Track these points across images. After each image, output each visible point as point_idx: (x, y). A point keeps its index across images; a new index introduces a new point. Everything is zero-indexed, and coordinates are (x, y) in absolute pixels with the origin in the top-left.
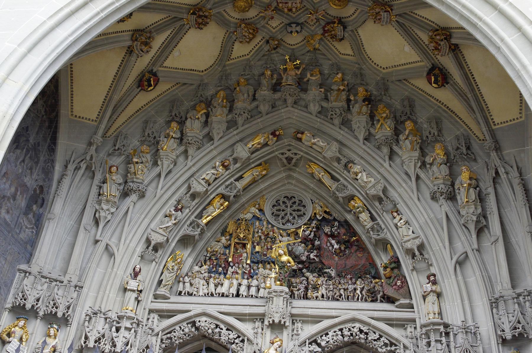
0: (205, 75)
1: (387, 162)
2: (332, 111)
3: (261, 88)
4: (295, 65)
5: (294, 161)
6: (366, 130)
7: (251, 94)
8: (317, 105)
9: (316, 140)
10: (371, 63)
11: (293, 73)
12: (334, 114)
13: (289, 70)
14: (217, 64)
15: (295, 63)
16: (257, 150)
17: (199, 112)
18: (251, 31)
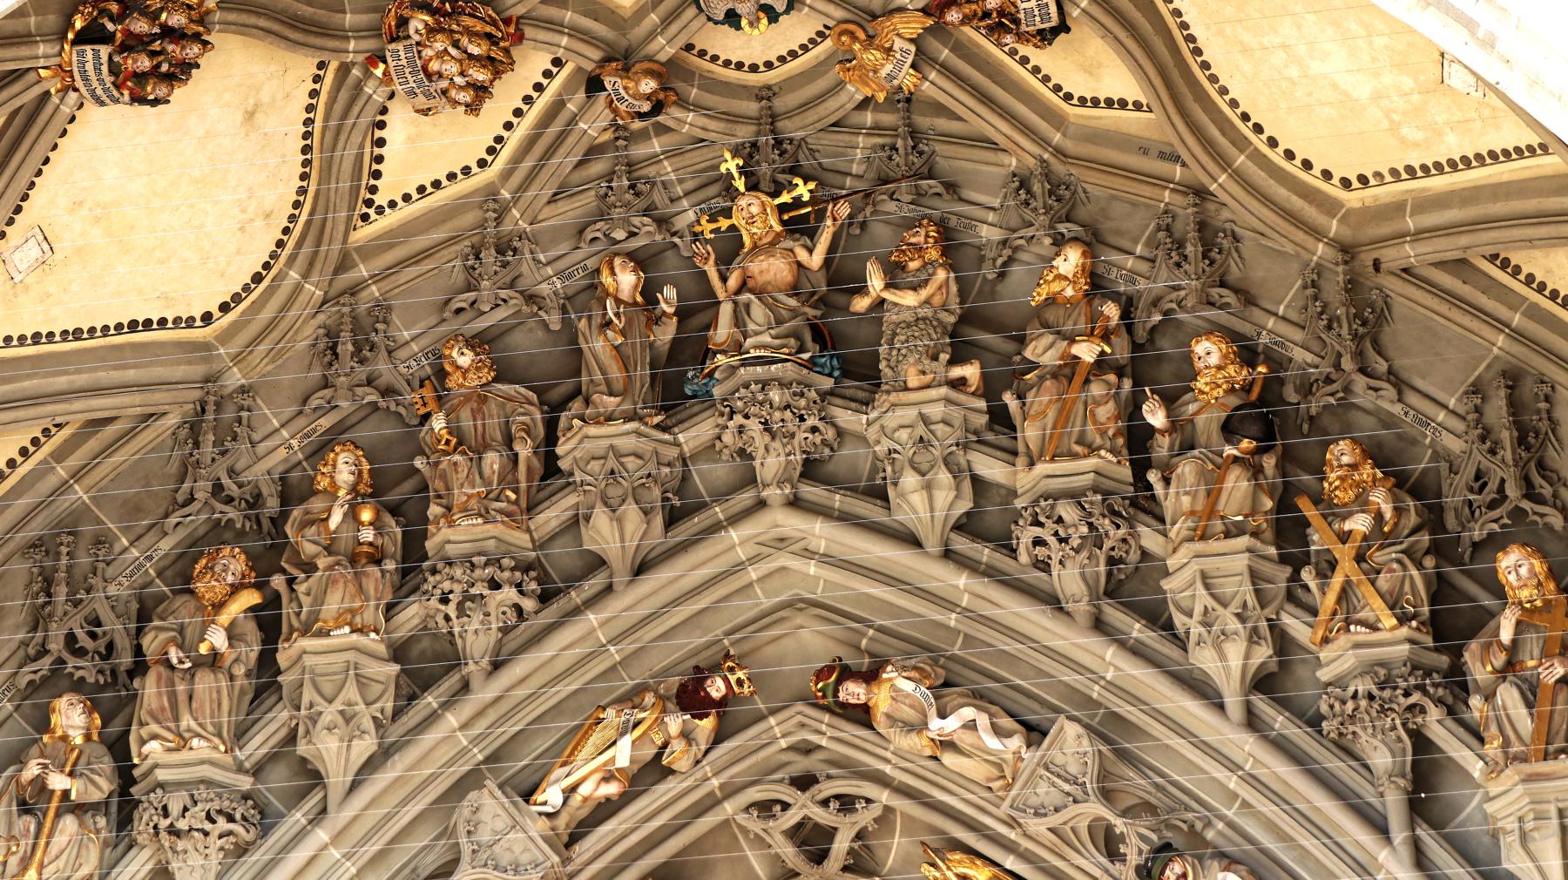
0: (225, 337)
1: (1399, 835)
2: (1037, 523)
3: (587, 402)
4: (782, 208)
5: (841, 845)
6: (1255, 630)
7: (524, 451)
8: (944, 476)
9: (952, 724)
10: (1265, 150)
11: (773, 269)
12: (1051, 540)
13: (755, 246)
14: (292, 259)
15: (785, 198)
16: (605, 810)
17: (219, 606)
18: (474, 50)
